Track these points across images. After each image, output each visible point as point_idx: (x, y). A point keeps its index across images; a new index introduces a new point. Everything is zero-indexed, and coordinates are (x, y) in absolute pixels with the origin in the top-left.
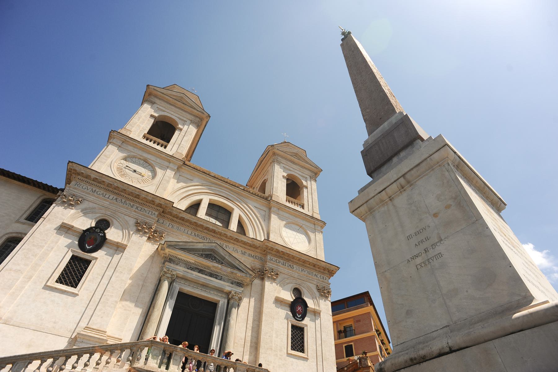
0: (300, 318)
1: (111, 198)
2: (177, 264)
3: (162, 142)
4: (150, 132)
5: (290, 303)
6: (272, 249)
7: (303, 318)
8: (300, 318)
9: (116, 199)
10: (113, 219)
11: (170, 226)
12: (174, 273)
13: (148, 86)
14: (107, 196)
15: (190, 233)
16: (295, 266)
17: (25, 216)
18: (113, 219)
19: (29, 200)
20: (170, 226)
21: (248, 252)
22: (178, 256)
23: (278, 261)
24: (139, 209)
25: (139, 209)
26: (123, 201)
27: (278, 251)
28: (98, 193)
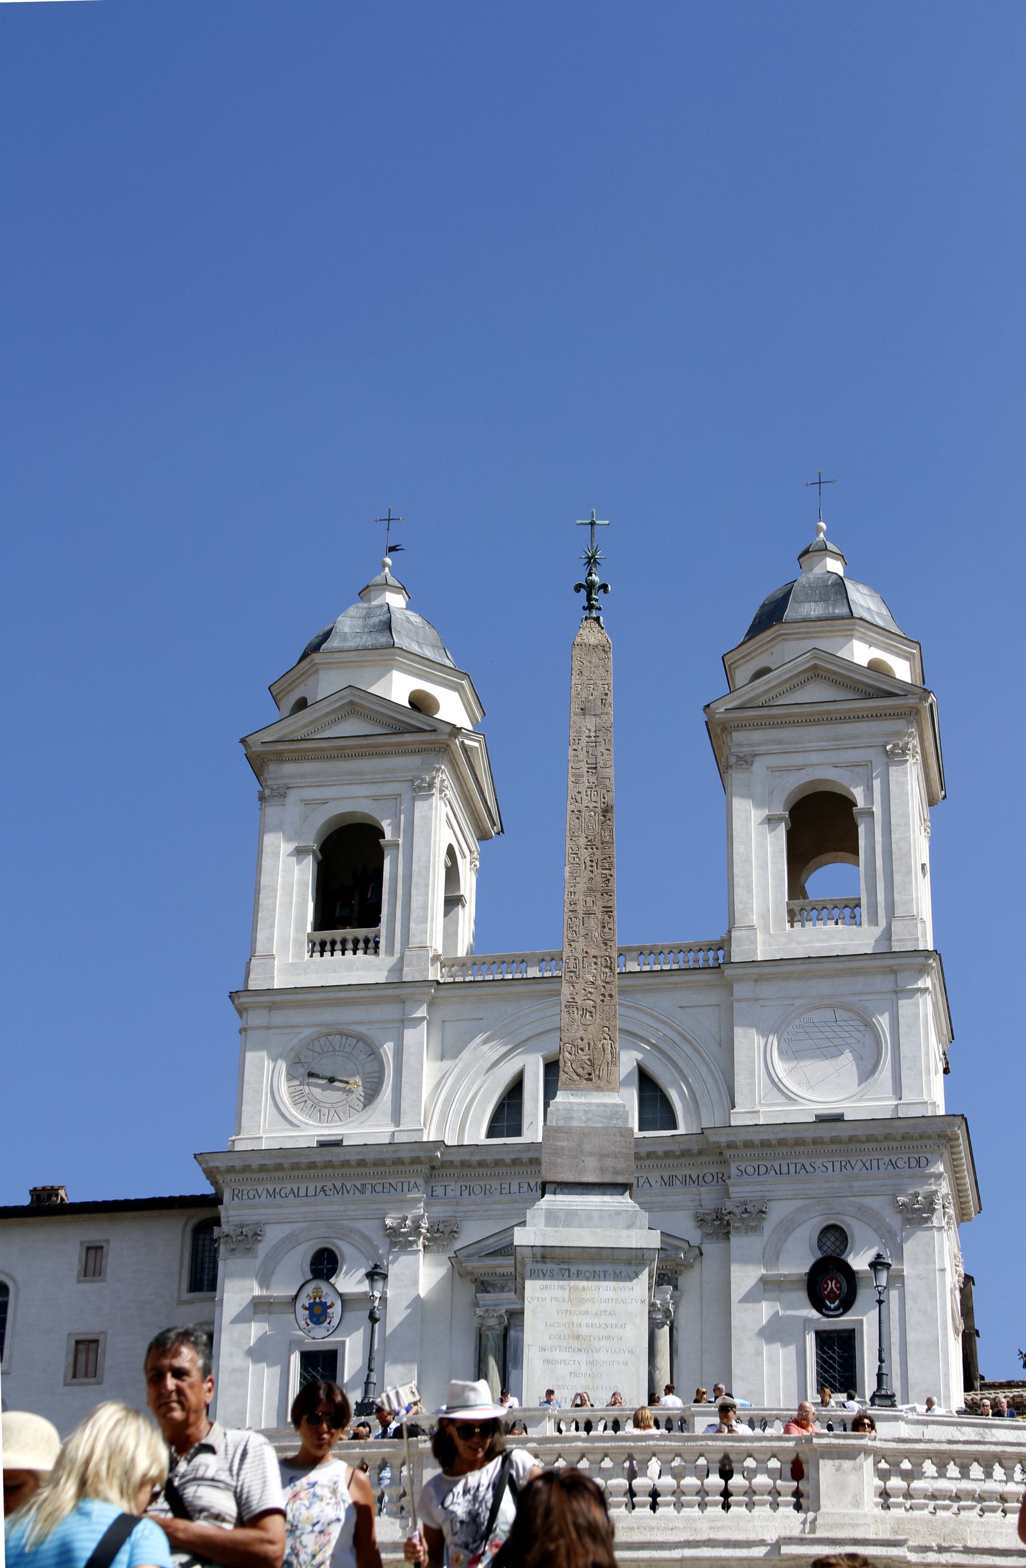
0: (836, 1309)
1: (311, 1192)
2: (502, 1289)
3: (361, 933)
4: (322, 922)
5: (806, 1278)
6: (731, 1145)
7: (847, 1303)
8: (836, 1309)
9: (323, 1189)
10: (336, 1241)
11: (466, 1193)
12: (500, 1313)
13: (243, 741)
14: (302, 1192)
15: (515, 1188)
16: (818, 1163)
17: (185, 1284)
18: (336, 1241)
19: (169, 1244)
20: (466, 1193)
21: (680, 1173)
22: (499, 1270)
23: (763, 1170)
24: (379, 1188)
25: (379, 1188)
26: (338, 1185)
27: (748, 1144)
28: (283, 1195)
